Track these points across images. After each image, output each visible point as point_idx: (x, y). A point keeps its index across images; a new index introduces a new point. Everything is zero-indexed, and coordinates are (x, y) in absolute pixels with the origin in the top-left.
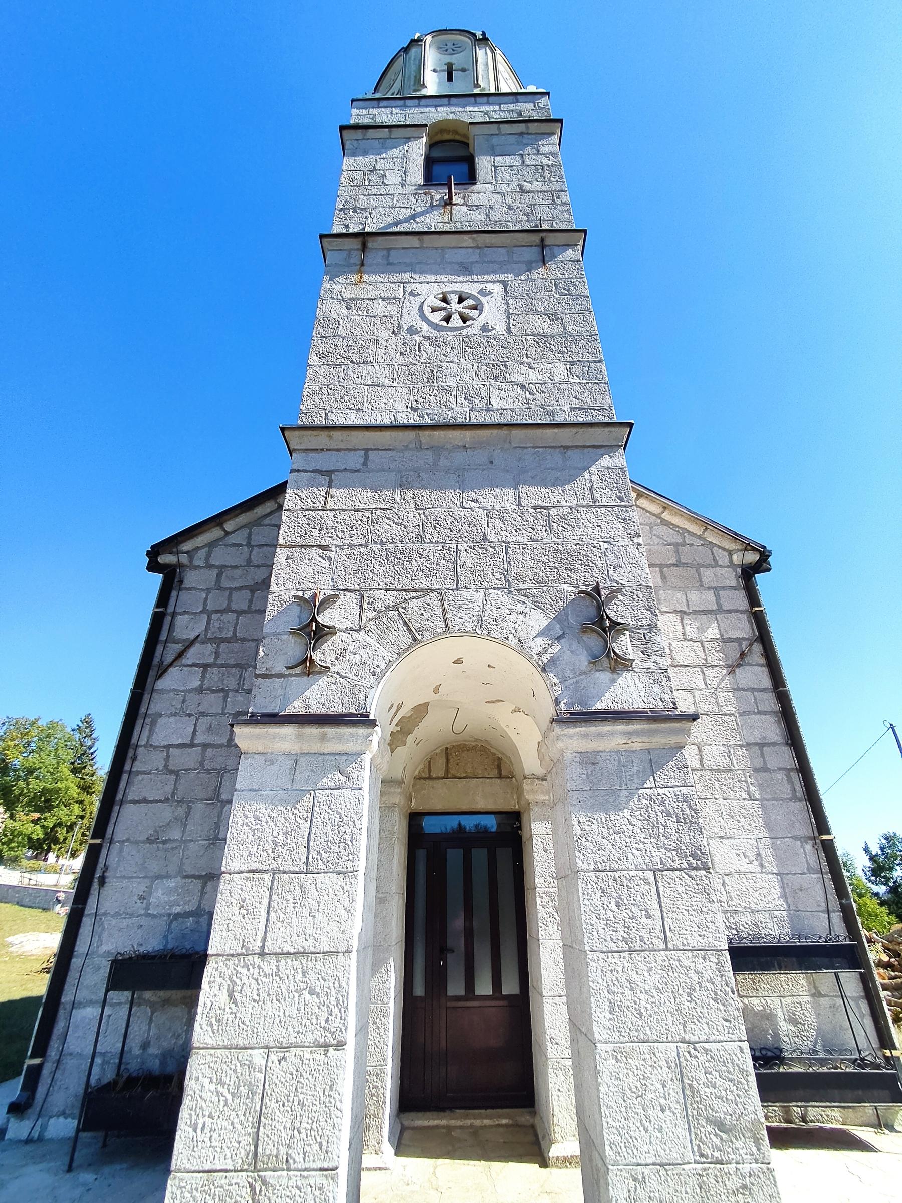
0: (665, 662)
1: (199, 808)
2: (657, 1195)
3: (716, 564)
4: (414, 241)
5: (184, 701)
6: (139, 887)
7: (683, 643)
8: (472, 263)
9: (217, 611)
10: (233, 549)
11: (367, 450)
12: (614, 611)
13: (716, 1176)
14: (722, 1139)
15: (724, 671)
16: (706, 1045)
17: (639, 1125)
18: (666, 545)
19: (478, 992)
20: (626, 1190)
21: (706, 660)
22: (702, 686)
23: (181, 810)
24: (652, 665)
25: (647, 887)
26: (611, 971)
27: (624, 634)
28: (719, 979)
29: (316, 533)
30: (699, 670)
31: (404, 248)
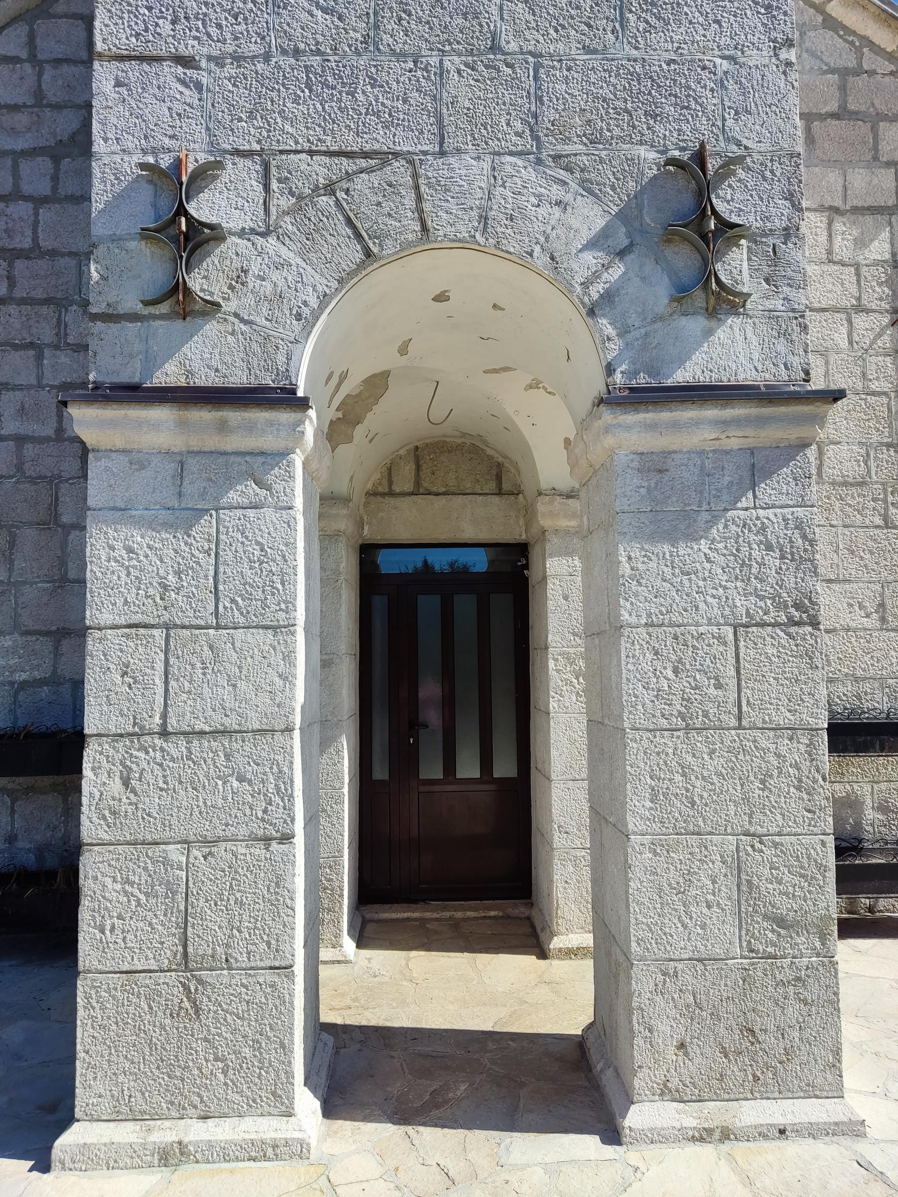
0: (801, 299)
1: (29, 536)
2: (690, 988)
7: (825, 268)
12: (727, 202)
13: (765, 970)
14: (779, 935)
15: (886, 320)
16: (777, 839)
17: (676, 921)
19: (461, 774)
20: (652, 984)
22: (844, 344)
24: (778, 304)
25: (721, 649)
26: (658, 754)
27: (738, 246)
28: (808, 764)
29: (166, 27)
30: (844, 316)
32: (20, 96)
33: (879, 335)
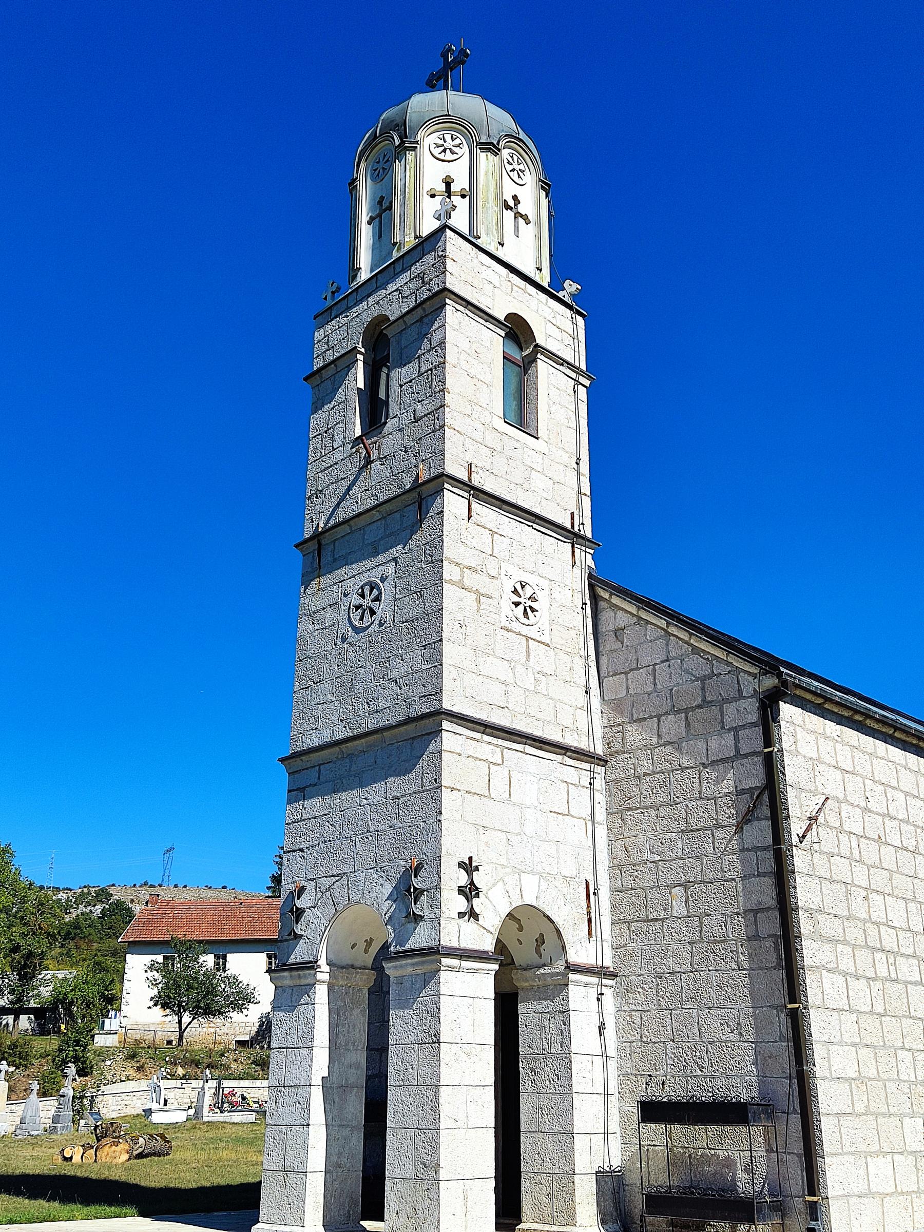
3: (741, 697)
4: (346, 528)
7: (698, 803)
11: (319, 765)
18: (693, 681)
21: (716, 820)
22: (711, 850)
30: (710, 832)
33: (730, 841)
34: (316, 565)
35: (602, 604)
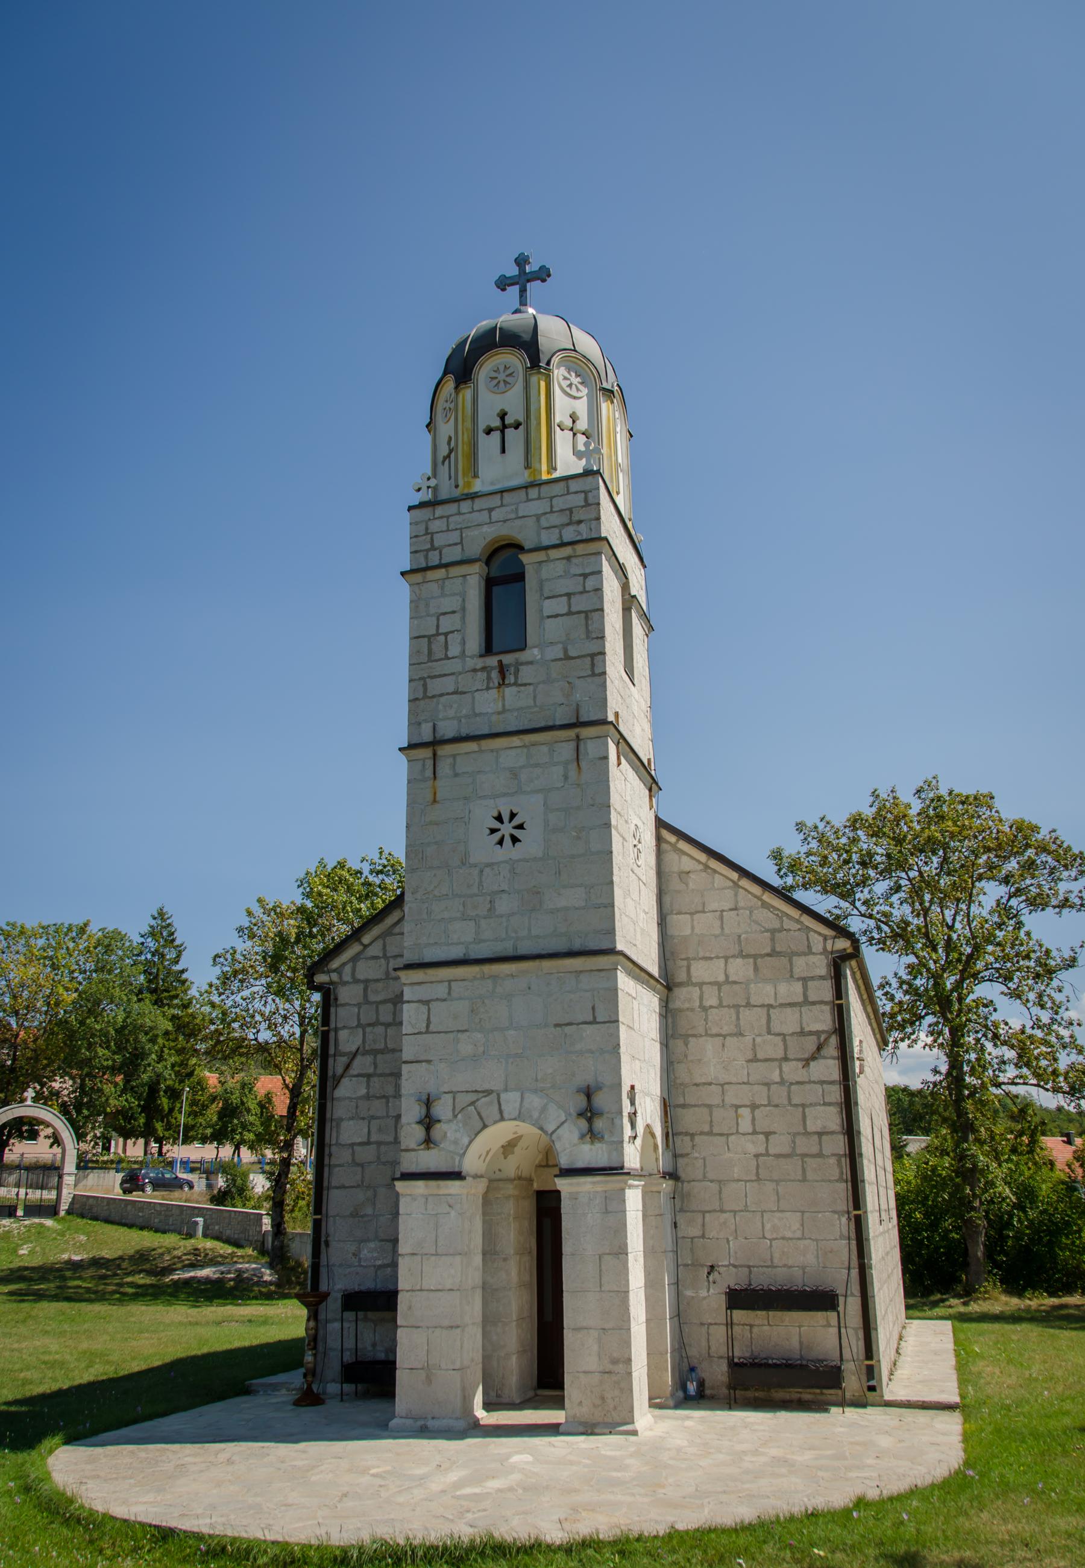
1: (382, 1191)
3: (809, 952)
5: (357, 1107)
6: (352, 1248)
8: (521, 767)
9: (369, 1025)
10: (372, 962)
11: (450, 981)
23: (370, 1193)
31: (466, 753)
32: (380, 974)
34: (429, 773)
35: (664, 846)
